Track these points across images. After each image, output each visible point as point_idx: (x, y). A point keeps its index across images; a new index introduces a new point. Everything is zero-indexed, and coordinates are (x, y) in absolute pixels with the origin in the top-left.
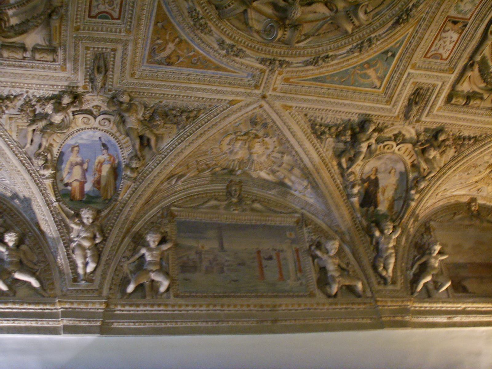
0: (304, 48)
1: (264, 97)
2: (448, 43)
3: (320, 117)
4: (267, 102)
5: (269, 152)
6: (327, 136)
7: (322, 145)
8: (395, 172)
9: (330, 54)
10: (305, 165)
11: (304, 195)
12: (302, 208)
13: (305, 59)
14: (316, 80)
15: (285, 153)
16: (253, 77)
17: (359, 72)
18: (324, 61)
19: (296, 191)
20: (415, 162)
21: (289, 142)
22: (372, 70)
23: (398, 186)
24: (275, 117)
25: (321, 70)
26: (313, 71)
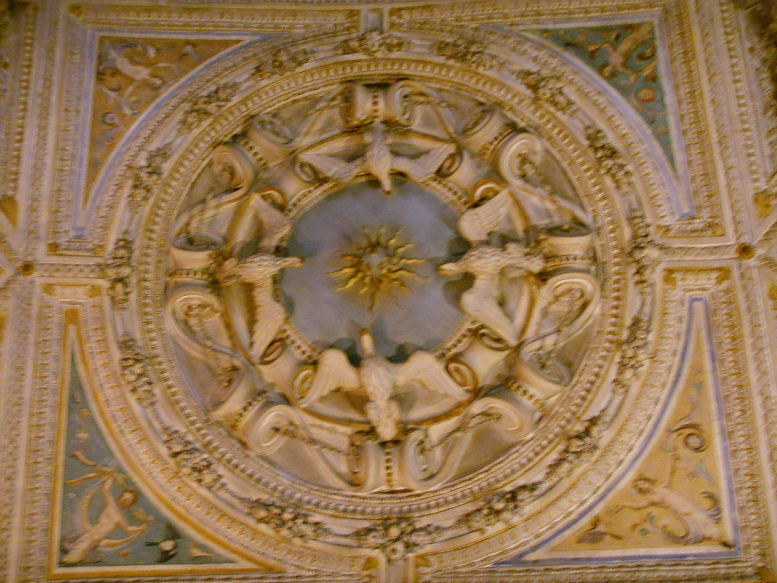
9: (157, 391)
14: (76, 386)
16: (79, 237)
17: (108, 485)
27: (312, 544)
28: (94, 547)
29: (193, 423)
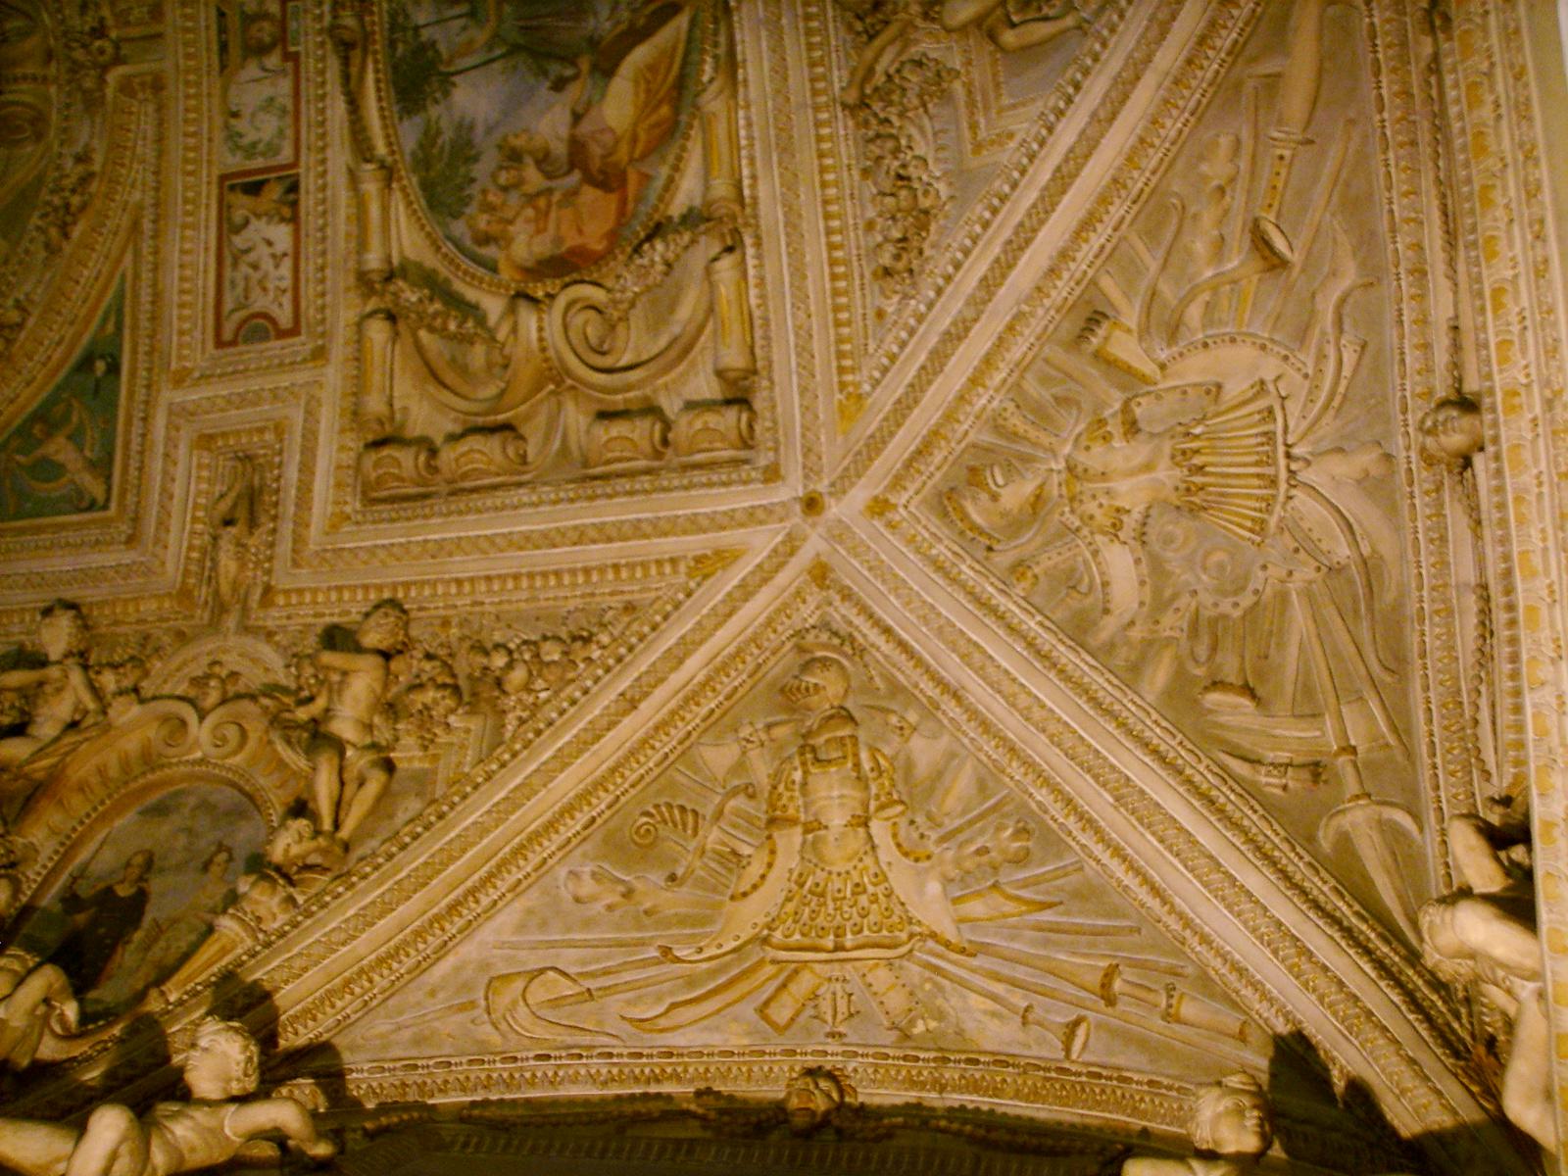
8: (231, 859)
27: (96, 168)
28: (90, 465)
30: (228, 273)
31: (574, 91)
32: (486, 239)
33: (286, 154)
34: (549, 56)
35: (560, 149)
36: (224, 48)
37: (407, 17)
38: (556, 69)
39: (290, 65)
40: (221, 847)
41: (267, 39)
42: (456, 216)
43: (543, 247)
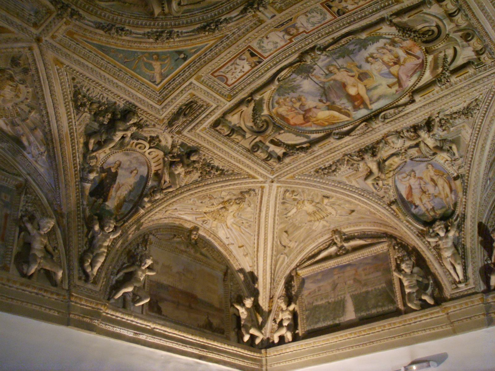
0: (103, 9)
1: (38, 40)
2: (238, 70)
3: (87, 88)
4: (40, 47)
5: (18, 100)
6: (86, 110)
7: (77, 118)
8: (137, 173)
9: (127, 28)
10: (50, 130)
11: (36, 161)
12: (29, 174)
13: (99, 20)
15: (34, 109)
16: (37, 12)
17: (145, 59)
18: (117, 32)
19: (29, 153)
20: (160, 172)
21: (44, 99)
22: (158, 63)
23: (134, 188)
24: (41, 66)
25: (110, 40)
26: (101, 37)
28: (161, 74)
29: (150, 25)
30: (229, 64)
31: (321, 104)
32: (278, 103)
33: (265, 55)
34: (326, 95)
35: (307, 107)
36: (282, 25)
37: (317, 61)
38: (324, 99)
39: (289, 41)
40: (136, 169)
41: (291, 33)
42: (279, 95)
43: (284, 113)
